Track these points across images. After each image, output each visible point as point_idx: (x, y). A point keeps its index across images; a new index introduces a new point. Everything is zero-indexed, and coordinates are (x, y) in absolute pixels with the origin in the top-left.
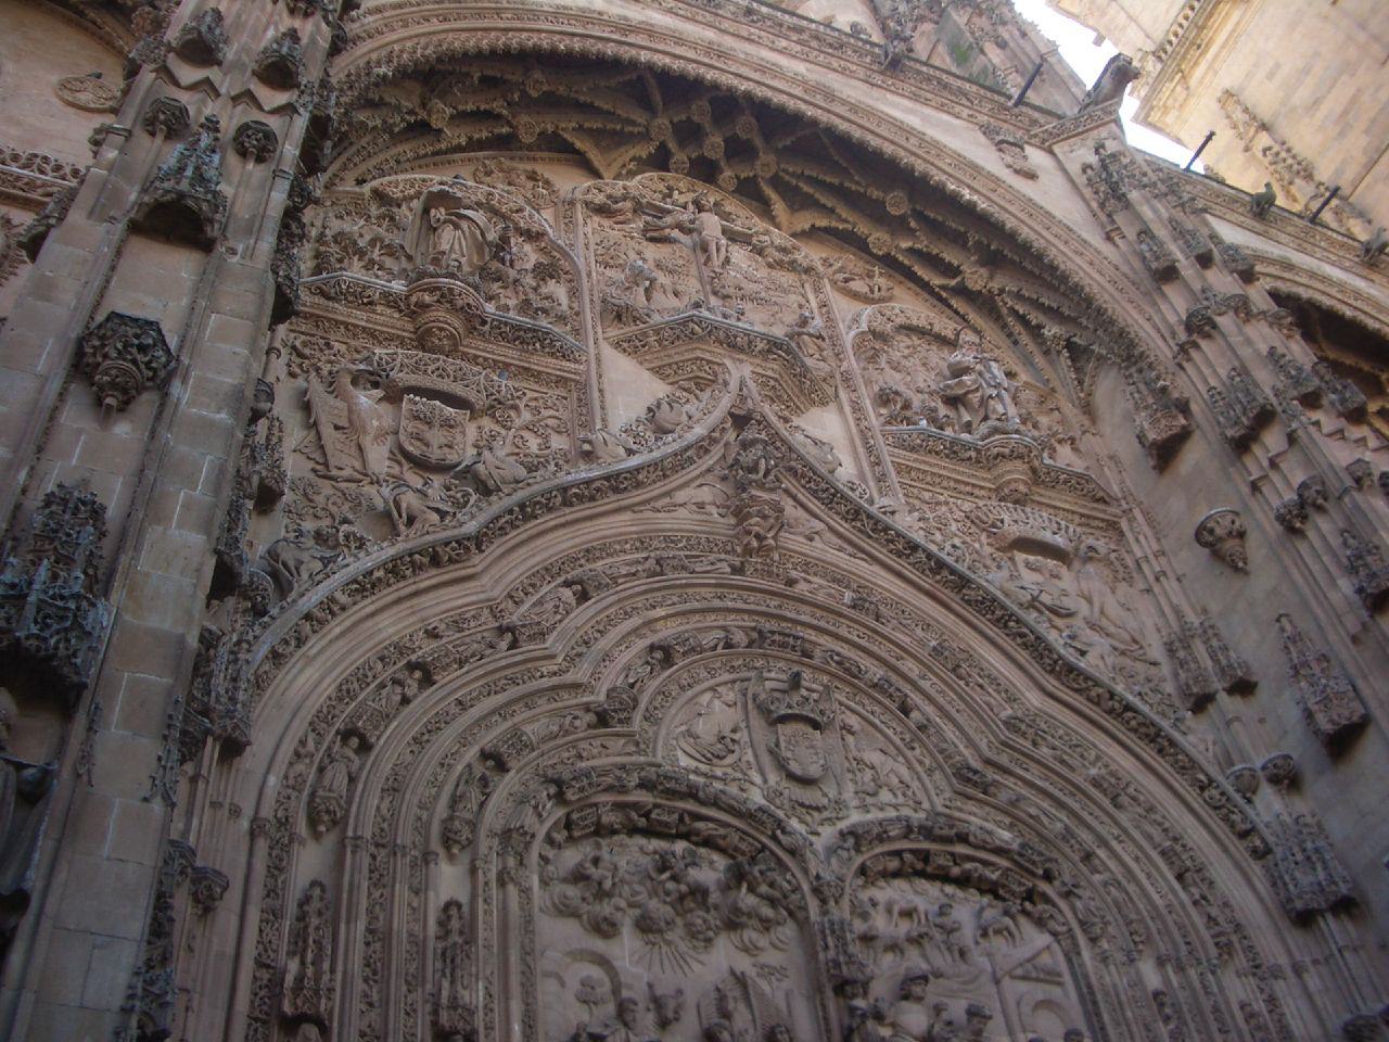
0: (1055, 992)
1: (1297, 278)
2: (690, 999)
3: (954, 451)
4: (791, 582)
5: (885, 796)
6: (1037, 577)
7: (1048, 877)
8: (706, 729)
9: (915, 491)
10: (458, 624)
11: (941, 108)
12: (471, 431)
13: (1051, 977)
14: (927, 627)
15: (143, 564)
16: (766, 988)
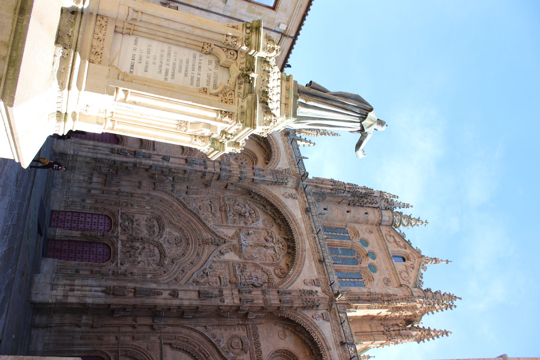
0: (147, 265)
1: (327, 352)
2: (140, 227)
3: (235, 271)
4: (199, 246)
5: (169, 250)
6: (215, 281)
7: (161, 266)
8: (172, 231)
9: (226, 266)
10: (178, 210)
11: (319, 273)
12: (209, 213)
13: (148, 266)
14: (198, 261)
15: (148, 161)
16: (143, 235)
